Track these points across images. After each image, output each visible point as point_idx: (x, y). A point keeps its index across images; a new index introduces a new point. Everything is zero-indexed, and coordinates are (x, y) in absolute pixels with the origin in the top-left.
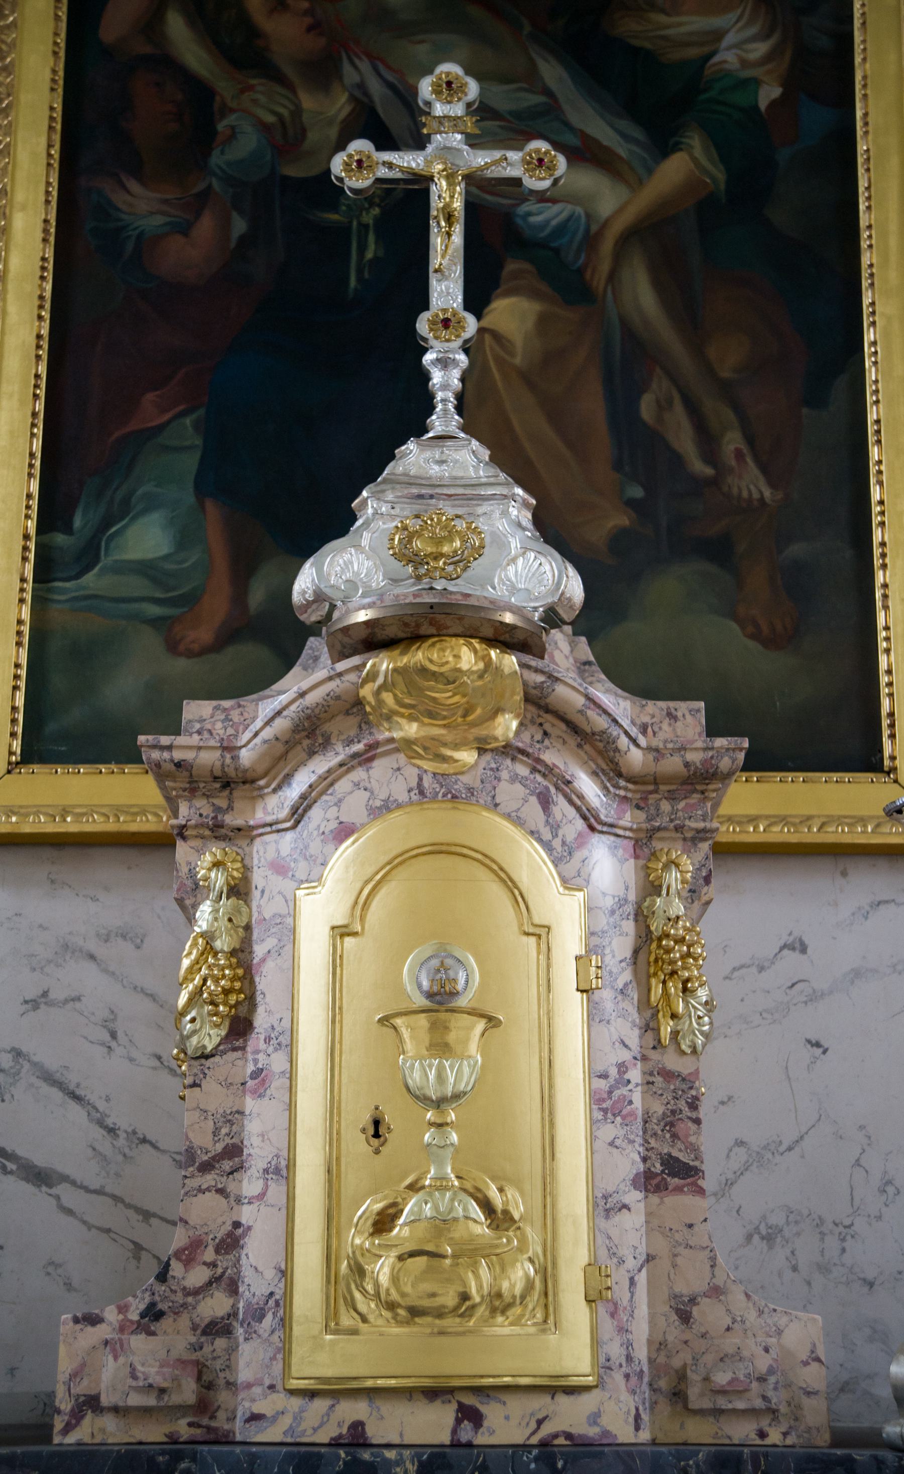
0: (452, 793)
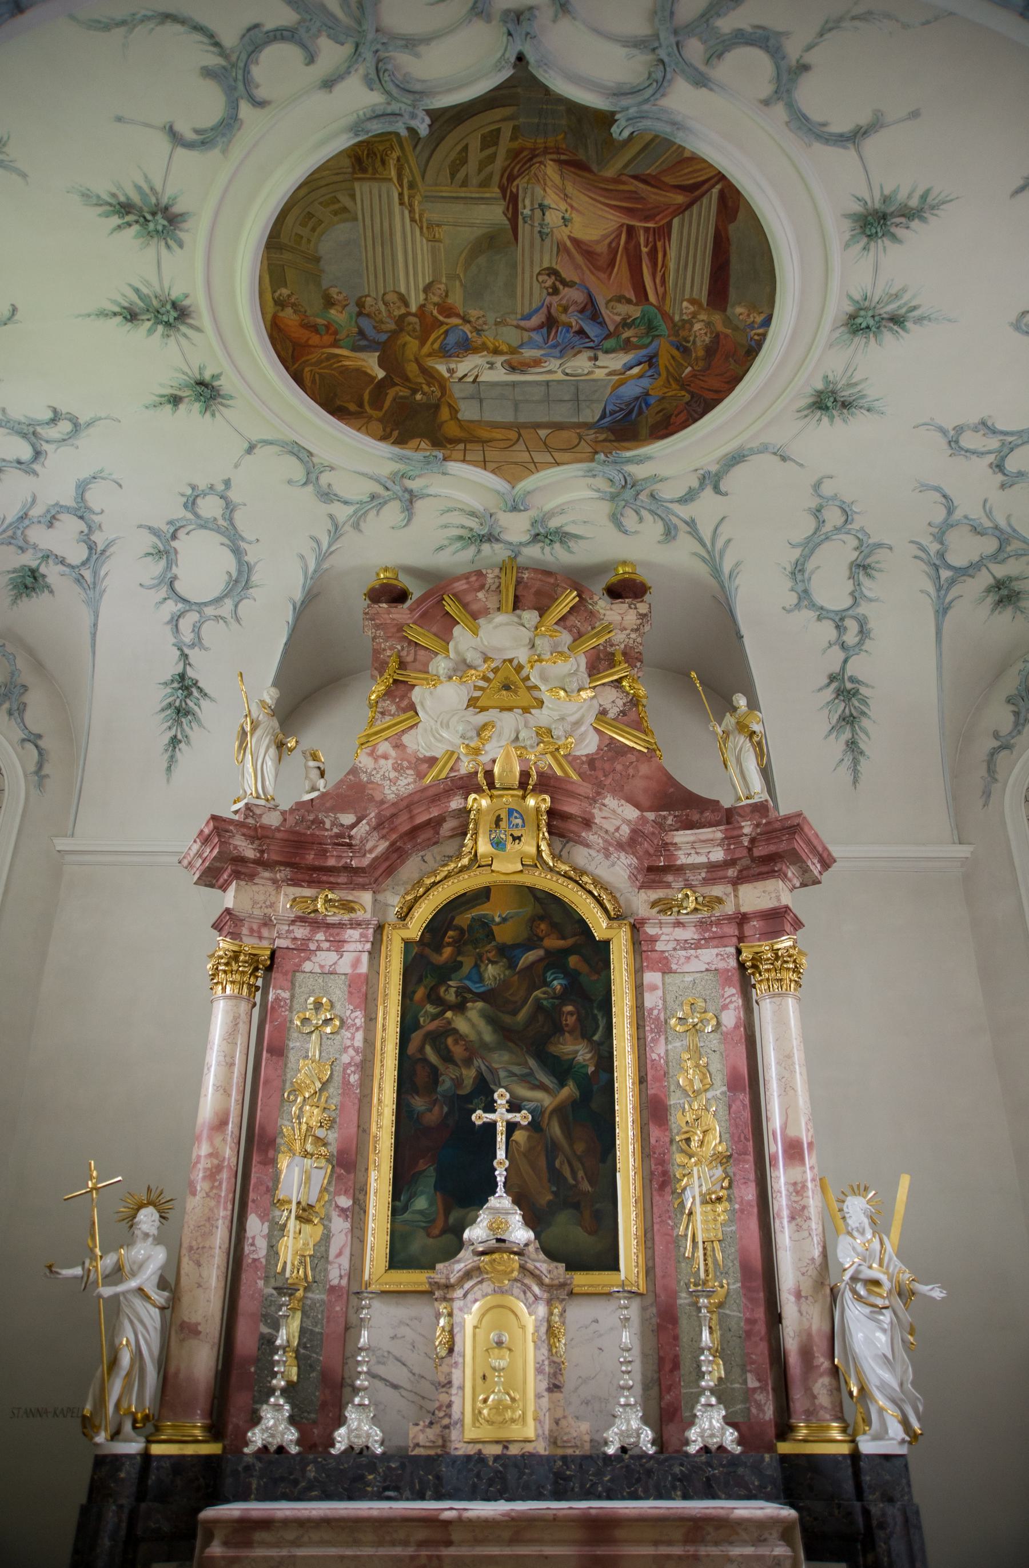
0: (502, 1291)
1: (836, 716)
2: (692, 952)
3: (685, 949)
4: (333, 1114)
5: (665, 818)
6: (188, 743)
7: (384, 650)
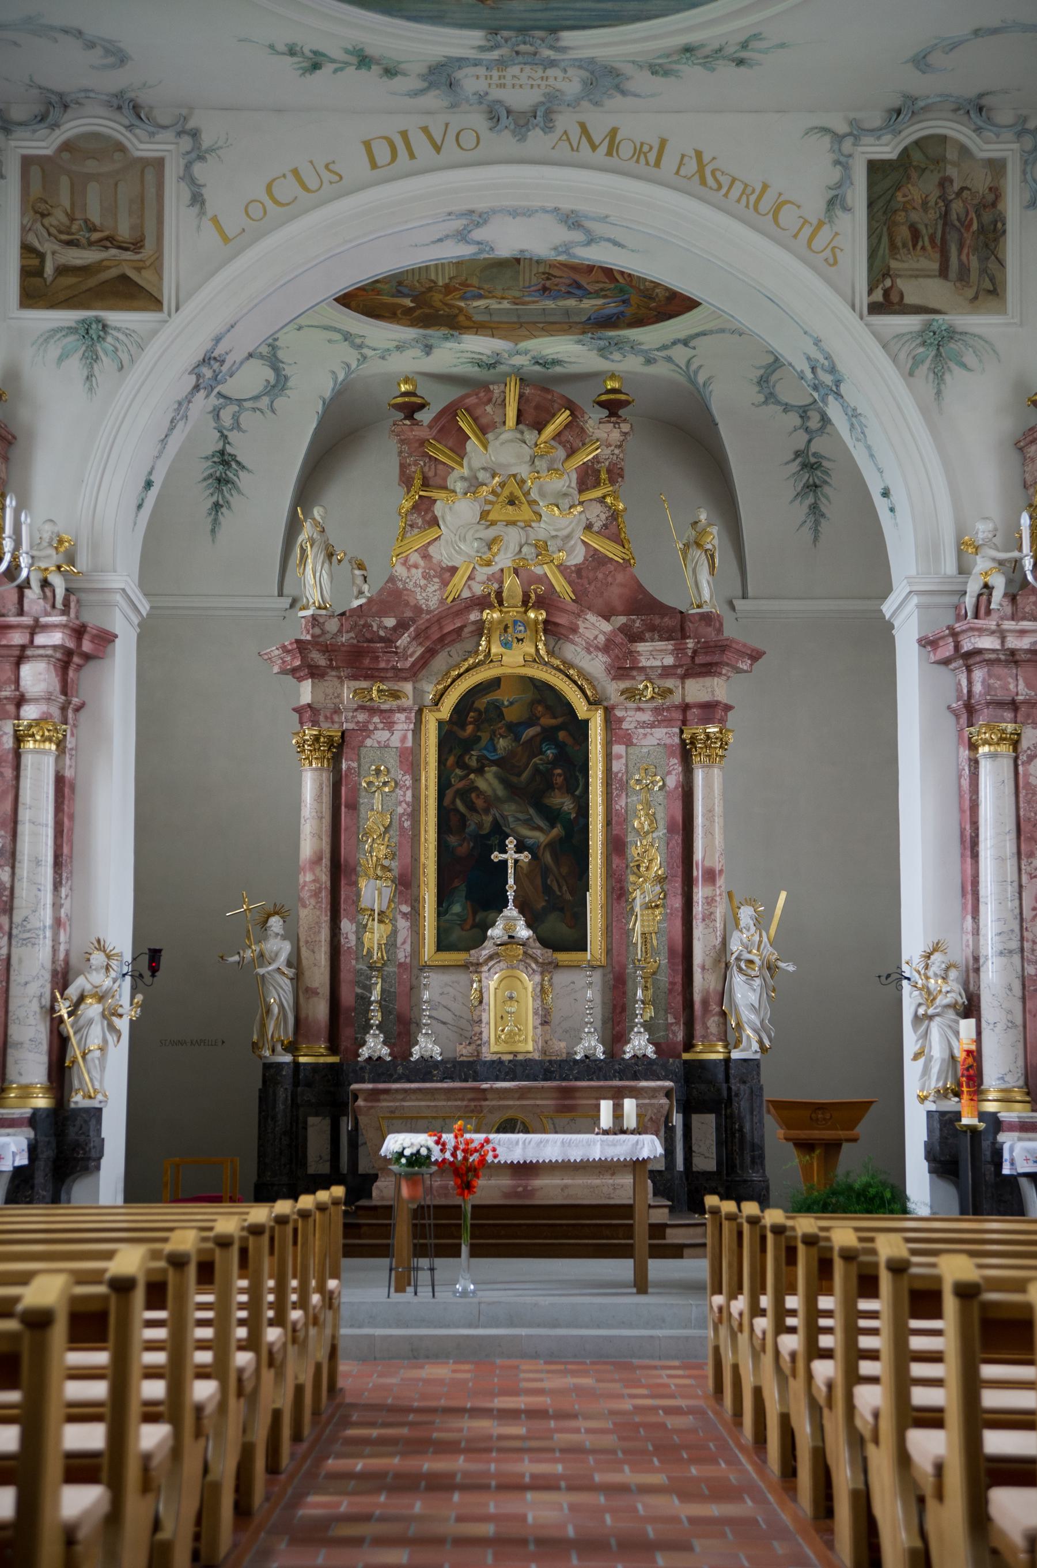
0: (512, 968)
1: (802, 485)
2: (649, 730)
3: (643, 728)
4: (394, 849)
5: (634, 621)
6: (229, 508)
7: (409, 465)
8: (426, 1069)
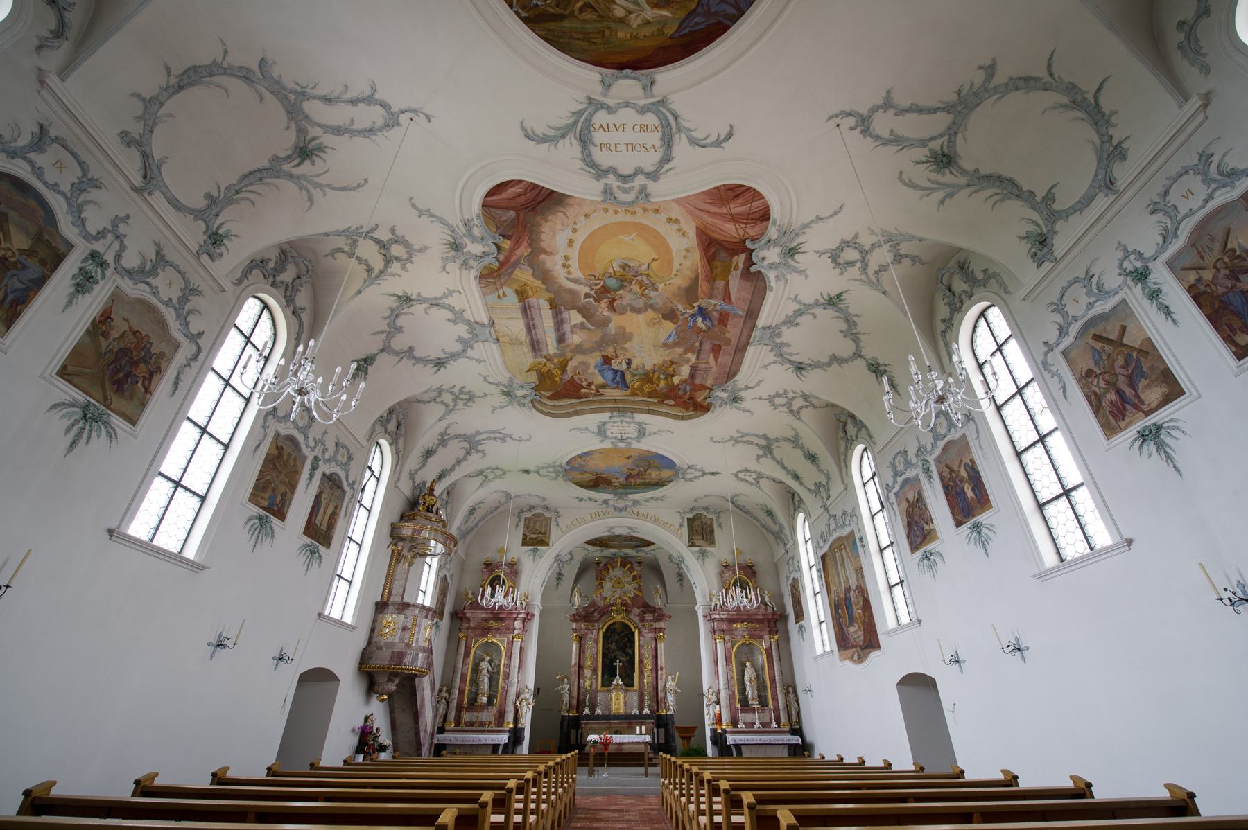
8: (598, 717)
